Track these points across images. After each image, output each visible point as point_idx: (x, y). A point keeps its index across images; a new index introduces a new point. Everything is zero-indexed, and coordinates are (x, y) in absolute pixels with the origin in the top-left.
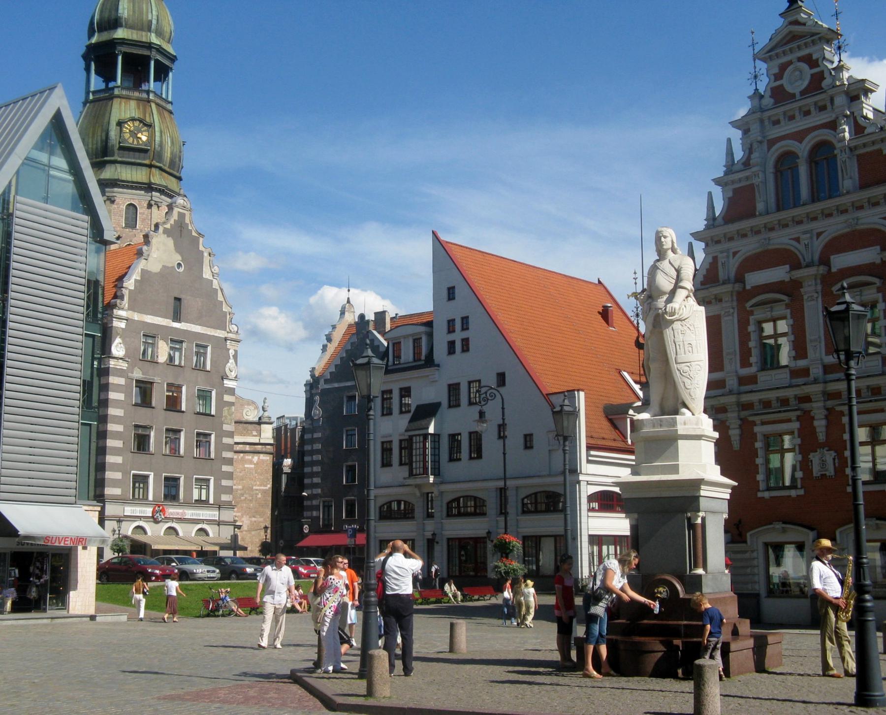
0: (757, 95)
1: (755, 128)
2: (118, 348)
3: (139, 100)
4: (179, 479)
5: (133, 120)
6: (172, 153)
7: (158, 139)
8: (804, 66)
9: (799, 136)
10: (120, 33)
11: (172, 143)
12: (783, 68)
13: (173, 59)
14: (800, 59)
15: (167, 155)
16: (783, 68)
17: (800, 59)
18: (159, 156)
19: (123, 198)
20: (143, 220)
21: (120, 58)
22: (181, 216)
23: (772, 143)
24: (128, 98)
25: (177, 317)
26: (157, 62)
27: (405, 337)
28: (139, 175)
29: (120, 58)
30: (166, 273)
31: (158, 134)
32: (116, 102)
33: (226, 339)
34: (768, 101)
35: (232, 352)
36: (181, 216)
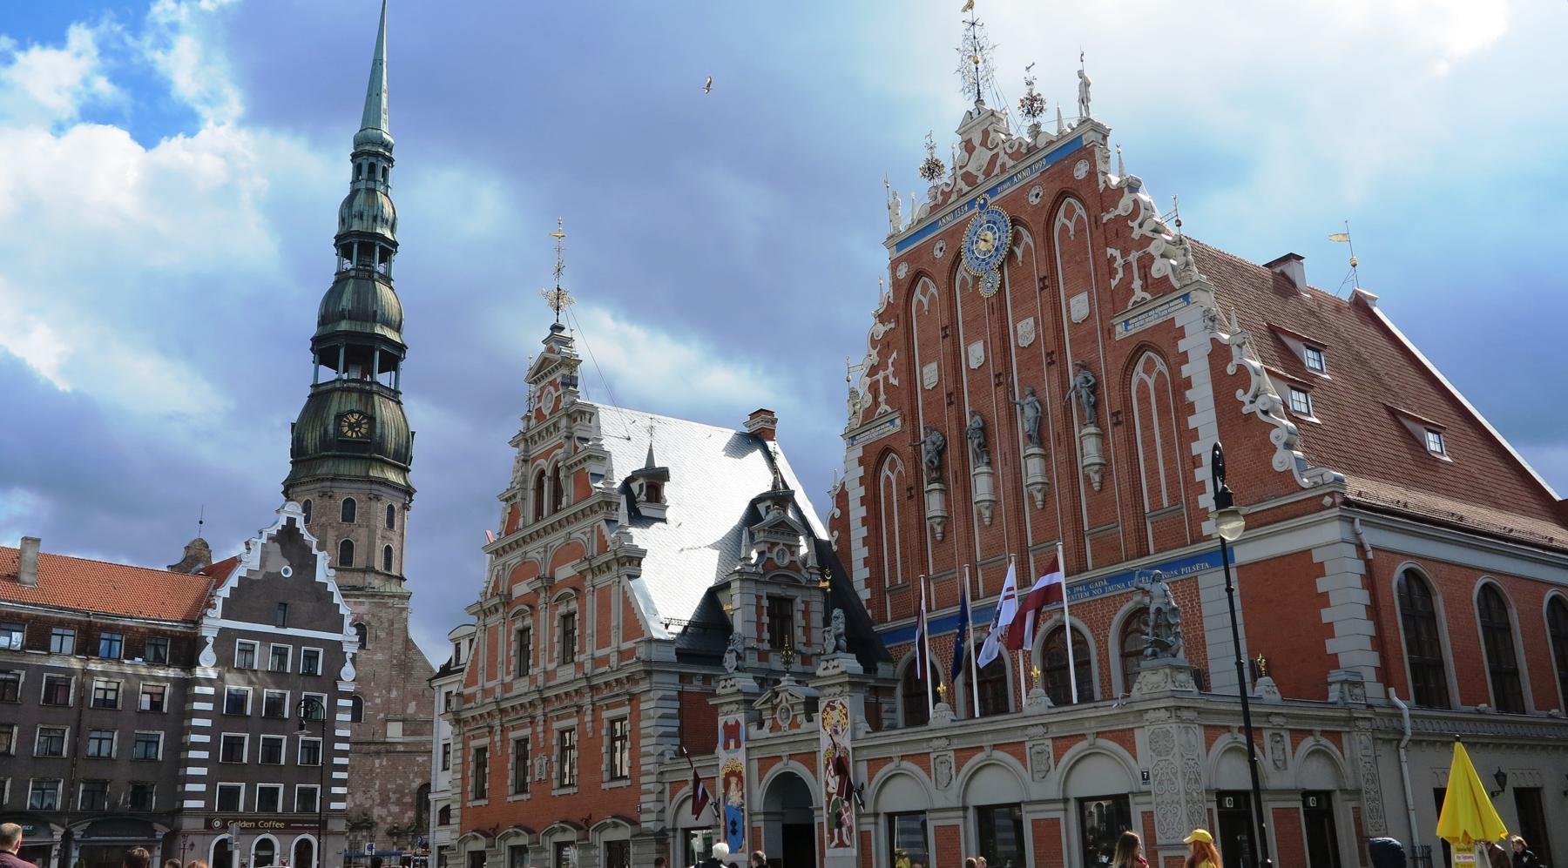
0: (528, 418)
1: (522, 446)
2: (207, 658)
3: (361, 391)
4: (277, 789)
5: (352, 412)
6: (397, 444)
7: (378, 431)
8: (552, 389)
9: (546, 455)
10: (344, 326)
11: (398, 434)
12: (542, 389)
13: (401, 348)
14: (551, 383)
15: (391, 446)
16: (542, 389)
17: (551, 383)
18: (380, 447)
19: (342, 493)
20: (362, 515)
21: (342, 352)
22: (291, 521)
23: (534, 460)
24: (350, 390)
25: (284, 626)
26: (382, 352)
27: (463, 637)
28: (355, 469)
29: (342, 352)
30: (273, 579)
31: (378, 426)
32: (336, 396)
33: (340, 643)
34: (533, 422)
35: (349, 656)
36: (291, 521)
